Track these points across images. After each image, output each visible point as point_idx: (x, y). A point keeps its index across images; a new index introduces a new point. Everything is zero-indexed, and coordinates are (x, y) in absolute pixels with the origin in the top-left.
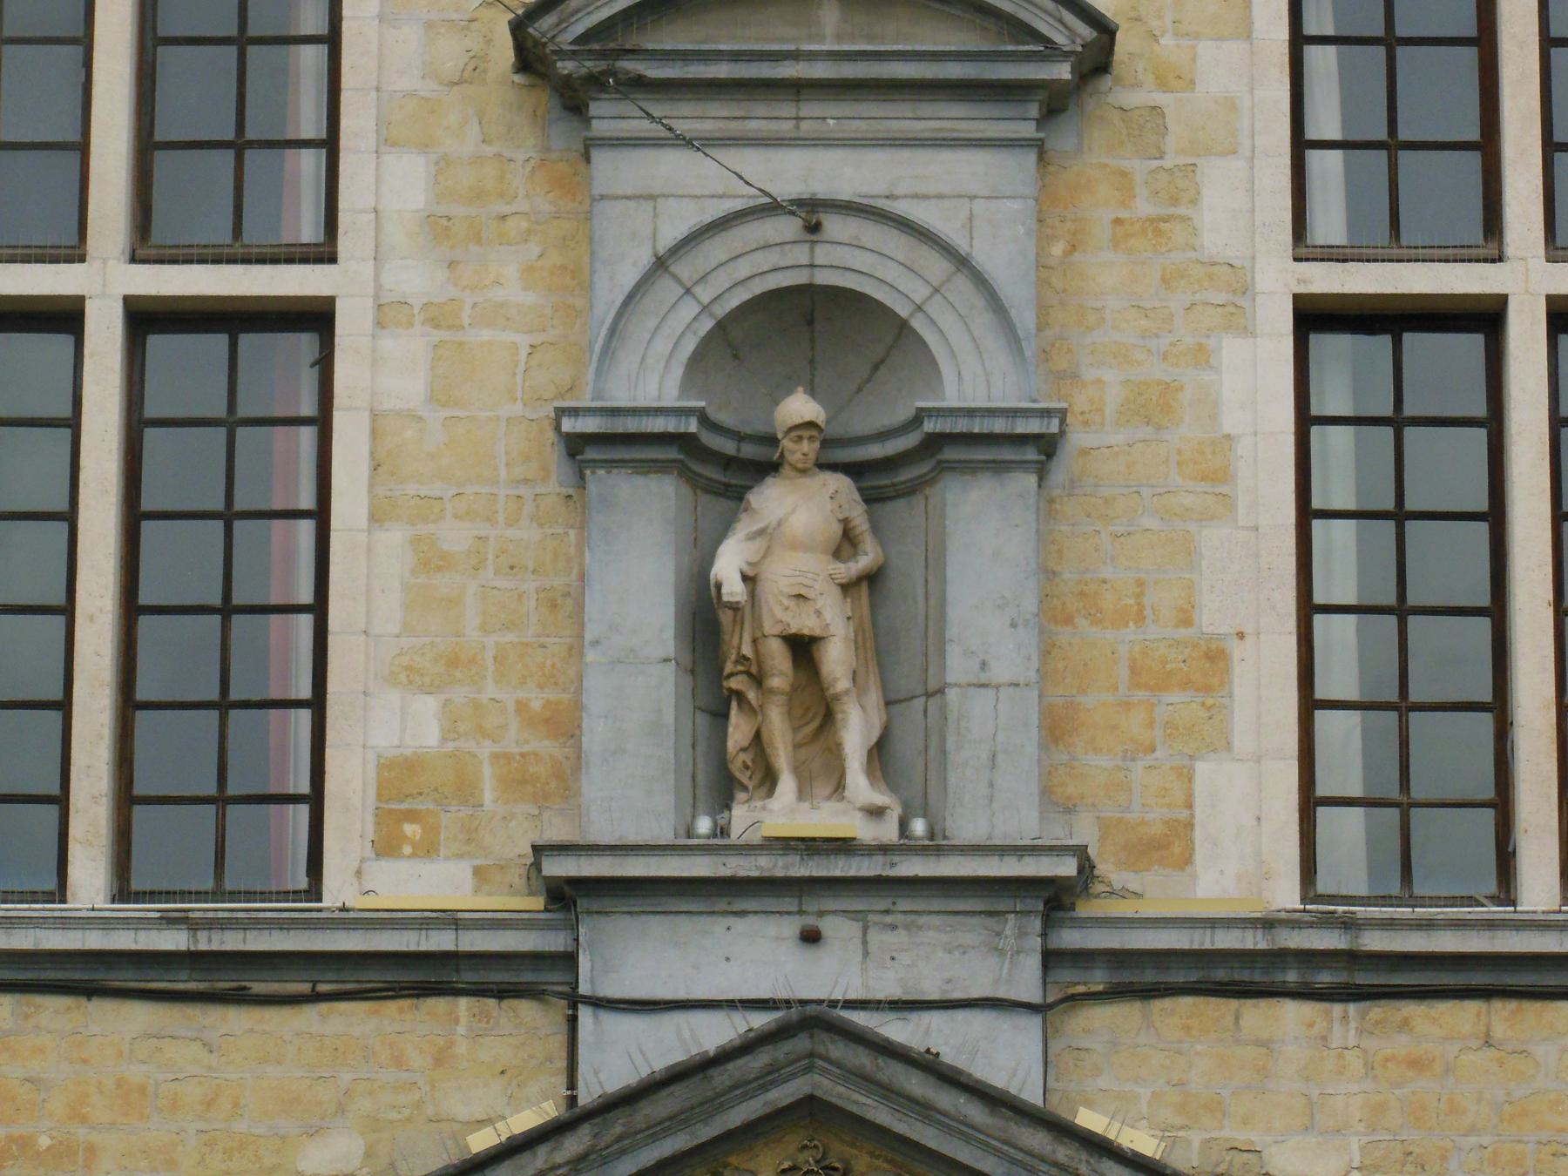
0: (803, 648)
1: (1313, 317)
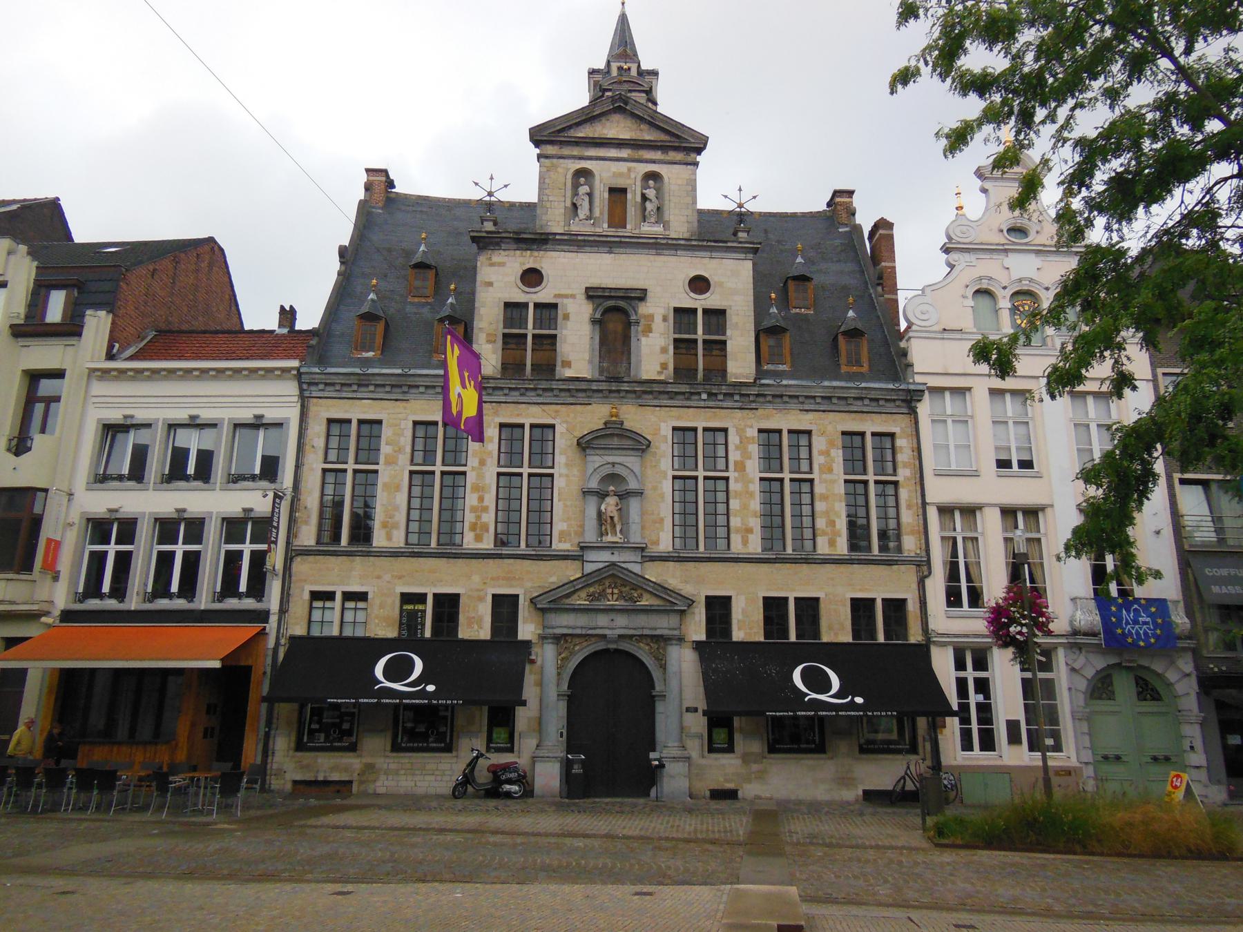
0: (612, 518)
1: (674, 477)
